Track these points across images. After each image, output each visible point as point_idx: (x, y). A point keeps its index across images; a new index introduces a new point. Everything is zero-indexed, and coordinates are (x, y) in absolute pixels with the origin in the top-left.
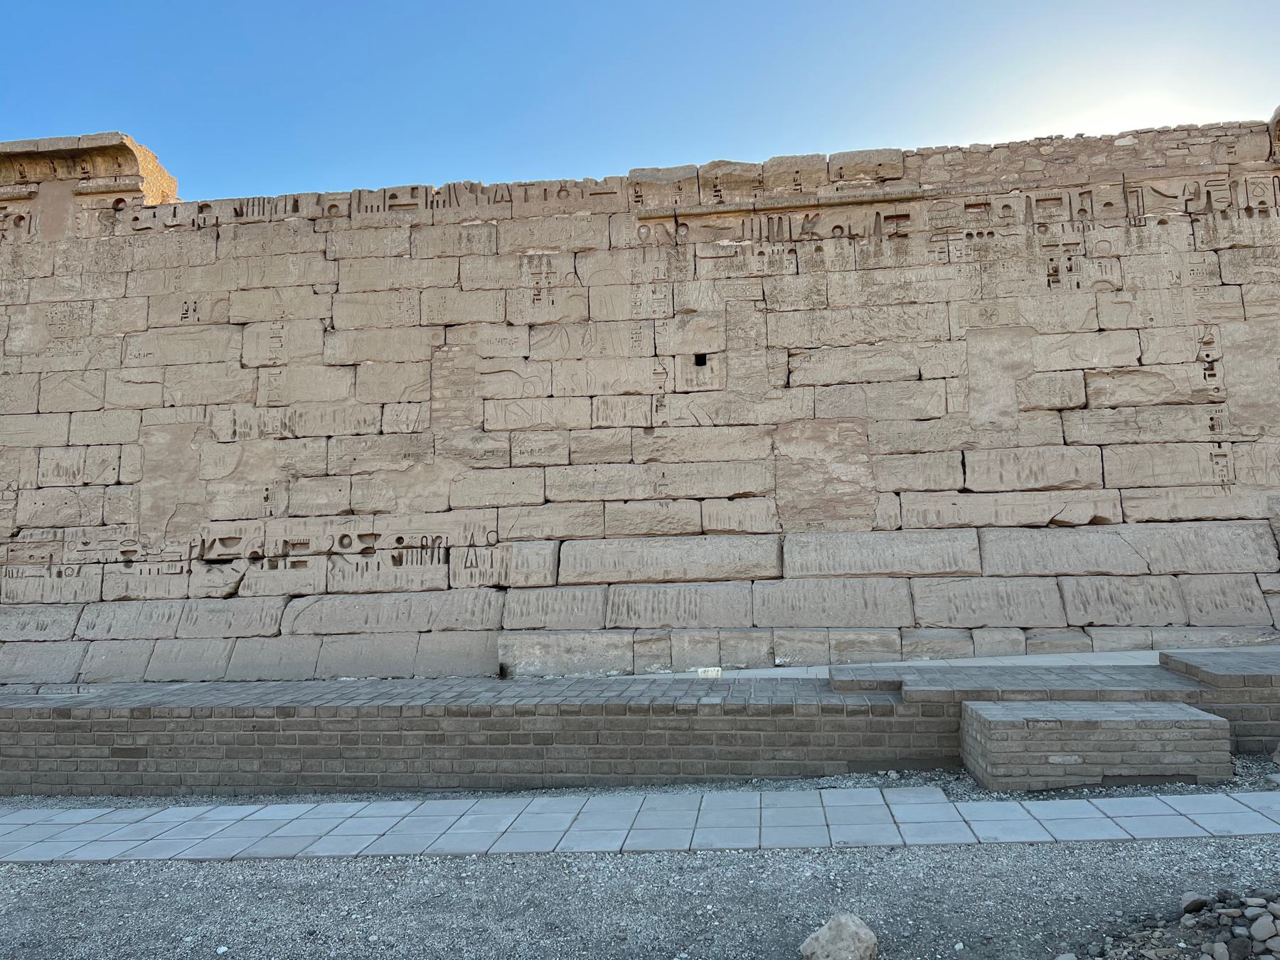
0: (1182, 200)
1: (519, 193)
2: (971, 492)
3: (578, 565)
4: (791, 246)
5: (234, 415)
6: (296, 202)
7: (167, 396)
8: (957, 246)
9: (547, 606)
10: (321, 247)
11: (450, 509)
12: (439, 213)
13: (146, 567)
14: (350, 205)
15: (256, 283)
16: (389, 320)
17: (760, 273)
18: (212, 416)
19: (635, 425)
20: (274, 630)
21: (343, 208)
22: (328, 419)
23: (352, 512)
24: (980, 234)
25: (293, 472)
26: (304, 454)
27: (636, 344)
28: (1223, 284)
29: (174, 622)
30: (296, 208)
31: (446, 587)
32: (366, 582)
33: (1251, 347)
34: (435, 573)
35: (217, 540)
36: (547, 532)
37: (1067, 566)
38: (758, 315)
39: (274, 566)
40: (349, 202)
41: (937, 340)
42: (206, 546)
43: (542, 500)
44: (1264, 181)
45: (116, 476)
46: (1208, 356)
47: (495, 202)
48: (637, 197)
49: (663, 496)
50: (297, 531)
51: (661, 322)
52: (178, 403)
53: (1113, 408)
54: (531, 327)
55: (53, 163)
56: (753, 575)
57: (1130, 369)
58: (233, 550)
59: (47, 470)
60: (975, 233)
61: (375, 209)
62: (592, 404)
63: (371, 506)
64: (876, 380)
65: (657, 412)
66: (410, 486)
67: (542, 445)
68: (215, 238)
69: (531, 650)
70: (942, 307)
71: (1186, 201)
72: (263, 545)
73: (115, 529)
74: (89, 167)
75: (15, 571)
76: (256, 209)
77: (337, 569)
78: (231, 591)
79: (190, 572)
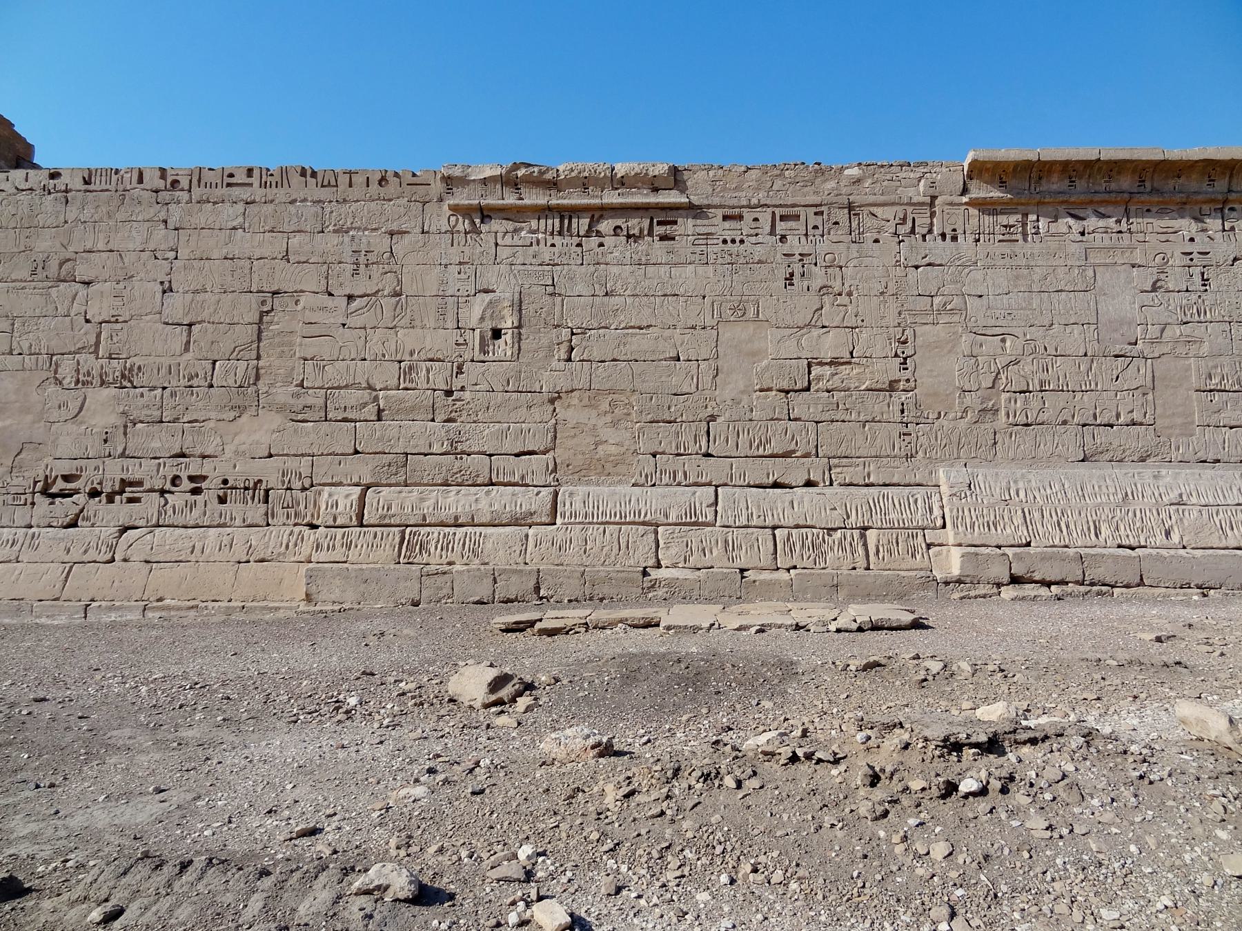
0: (892, 223)
1: (343, 180)
2: (713, 456)
3: (380, 510)
4: (576, 240)
7: (15, 345)
8: (715, 248)
9: (351, 541)
10: (162, 215)
11: (270, 456)
12: (271, 192)
14: (191, 181)
15: (101, 246)
16: (222, 285)
17: (551, 262)
18: (56, 364)
19: (437, 388)
20: (108, 557)
21: (184, 183)
22: (164, 371)
23: (183, 455)
24: (733, 241)
25: (132, 418)
26: (141, 401)
27: (441, 317)
28: (920, 295)
29: (16, 548)
30: (140, 181)
31: (265, 524)
32: (194, 516)
33: (937, 347)
34: (256, 511)
36: (356, 479)
37: (782, 520)
38: (548, 297)
39: (110, 500)
40: (190, 177)
41: (693, 328)
42: (49, 481)
43: (352, 451)
47: (322, 186)
48: (448, 189)
49: (459, 451)
50: (135, 473)
51: (464, 299)
52: (26, 351)
53: (828, 391)
54: (350, 298)
56: (529, 521)
57: (842, 360)
60: (729, 239)
61: (214, 185)
62: (400, 368)
63: (198, 451)
64: (642, 359)
65: (456, 377)
66: (236, 434)
67: (353, 402)
68: (64, 204)
69: (332, 581)
70: (701, 300)
72: (100, 483)
77: (168, 506)
78: (72, 522)
79: (33, 504)
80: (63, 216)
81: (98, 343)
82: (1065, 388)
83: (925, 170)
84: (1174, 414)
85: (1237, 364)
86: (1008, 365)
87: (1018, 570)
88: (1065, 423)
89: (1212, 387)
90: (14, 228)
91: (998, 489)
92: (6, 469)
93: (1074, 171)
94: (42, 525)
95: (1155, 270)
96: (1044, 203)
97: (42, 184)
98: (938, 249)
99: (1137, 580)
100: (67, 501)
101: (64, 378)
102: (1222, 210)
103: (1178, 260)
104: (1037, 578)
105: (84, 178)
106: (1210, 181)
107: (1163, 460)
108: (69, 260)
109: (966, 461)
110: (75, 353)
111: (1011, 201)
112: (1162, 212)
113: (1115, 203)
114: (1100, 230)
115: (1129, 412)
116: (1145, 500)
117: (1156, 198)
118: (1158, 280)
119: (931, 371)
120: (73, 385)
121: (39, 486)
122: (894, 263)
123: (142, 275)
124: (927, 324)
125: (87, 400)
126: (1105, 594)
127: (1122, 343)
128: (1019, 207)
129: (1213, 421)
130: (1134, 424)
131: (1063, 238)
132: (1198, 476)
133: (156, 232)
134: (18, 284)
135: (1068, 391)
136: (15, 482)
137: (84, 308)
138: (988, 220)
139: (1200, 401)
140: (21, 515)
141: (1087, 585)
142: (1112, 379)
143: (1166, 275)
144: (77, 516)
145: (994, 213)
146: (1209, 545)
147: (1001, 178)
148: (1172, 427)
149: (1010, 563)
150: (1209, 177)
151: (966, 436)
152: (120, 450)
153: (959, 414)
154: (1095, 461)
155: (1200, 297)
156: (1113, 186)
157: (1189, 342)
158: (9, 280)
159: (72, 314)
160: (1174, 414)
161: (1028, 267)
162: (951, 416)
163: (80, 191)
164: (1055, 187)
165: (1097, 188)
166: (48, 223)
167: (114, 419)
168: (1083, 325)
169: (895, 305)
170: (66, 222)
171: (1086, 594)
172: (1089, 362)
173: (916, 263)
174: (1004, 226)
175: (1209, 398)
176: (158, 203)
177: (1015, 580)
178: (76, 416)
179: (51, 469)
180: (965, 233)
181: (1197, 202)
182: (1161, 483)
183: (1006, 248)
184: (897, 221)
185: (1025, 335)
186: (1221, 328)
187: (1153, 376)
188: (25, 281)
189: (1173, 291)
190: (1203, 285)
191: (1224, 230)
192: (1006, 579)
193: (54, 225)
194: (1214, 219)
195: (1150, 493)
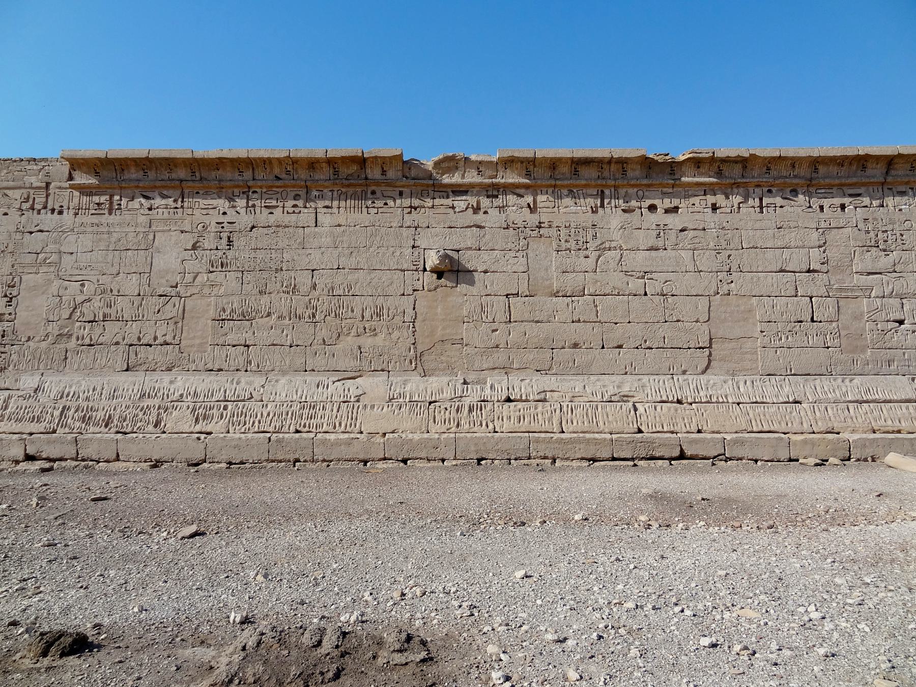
33: (35, 290)
44: (64, 193)
46: (11, 294)
71: (21, 202)
82: (120, 319)
83: (45, 164)
84: (195, 336)
85: (244, 301)
86: (83, 302)
87: (31, 451)
88: (117, 343)
89: (224, 317)
91: (55, 392)
93: (144, 165)
95: (197, 235)
96: (125, 188)
98: (48, 220)
99: (114, 456)
102: (249, 191)
103: (213, 228)
104: (44, 457)
106: (240, 172)
107: (183, 370)
109: (42, 371)
111: (98, 187)
112: (207, 194)
113: (173, 187)
114: (162, 207)
115: (163, 336)
116: (156, 398)
117: (197, 184)
118: (197, 242)
119: (28, 307)
122: (16, 229)
124: (31, 273)
126: (90, 467)
127: (166, 286)
128: (108, 190)
129: (220, 342)
130: (168, 344)
131: (135, 213)
132: (202, 381)
135: (123, 321)
138: (85, 199)
139: (213, 327)
141: (80, 461)
142: (155, 312)
143: (203, 238)
145: (91, 194)
146: (181, 431)
147: (95, 170)
148: (192, 346)
149: (26, 446)
150: (239, 169)
151: (45, 353)
153: (43, 338)
154: (136, 371)
155: (224, 253)
156: (174, 176)
157: (213, 285)
160: (195, 336)
161: (109, 233)
162: (37, 339)
164: (134, 176)
165: (163, 177)
168: (140, 274)
169: (11, 259)
171: (76, 467)
172: (140, 300)
173: (30, 230)
174: (96, 204)
175: (220, 325)
177: (29, 458)
180: (69, 209)
181: (230, 187)
182: (173, 386)
183: (95, 219)
184: (22, 200)
185: (98, 281)
186: (236, 275)
187: (184, 310)
189: (207, 250)
190: (228, 245)
191: (247, 207)
192: (21, 458)
194: (241, 199)
195: (161, 393)
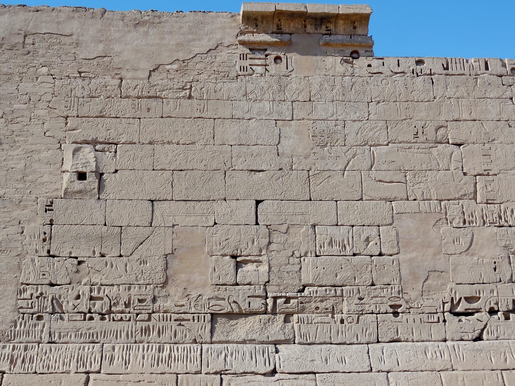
5: (463, 208)
6: (486, 63)
10: (508, 94)
13: (410, 317)
15: (465, 116)
30: (487, 68)
35: (463, 299)
45: (379, 249)
55: (305, 21)
58: (475, 305)
59: (324, 243)
73: (383, 288)
74: (331, 27)
75: (306, 319)
76: (458, 65)
79: (445, 321)
80: (432, 93)
81: (475, 192)
90: (395, 102)
92: (417, 293)
94: (456, 338)
97: (411, 68)
100: (473, 319)
101: (453, 219)
105: (443, 65)
108: (442, 127)
110: (459, 199)
120: (461, 225)
121: (447, 307)
123: (501, 139)
125: (475, 237)
133: (506, 106)
134: (405, 145)
136: (427, 303)
137: (461, 164)
140: (437, 331)
144: (482, 330)
152: (508, 277)
158: (396, 141)
159: (452, 168)
163: (442, 74)
166: (422, 97)
167: (499, 252)
170: (435, 98)
176: (503, 85)
178: (468, 249)
179: (455, 293)
188: (410, 143)
193: (426, 100)
